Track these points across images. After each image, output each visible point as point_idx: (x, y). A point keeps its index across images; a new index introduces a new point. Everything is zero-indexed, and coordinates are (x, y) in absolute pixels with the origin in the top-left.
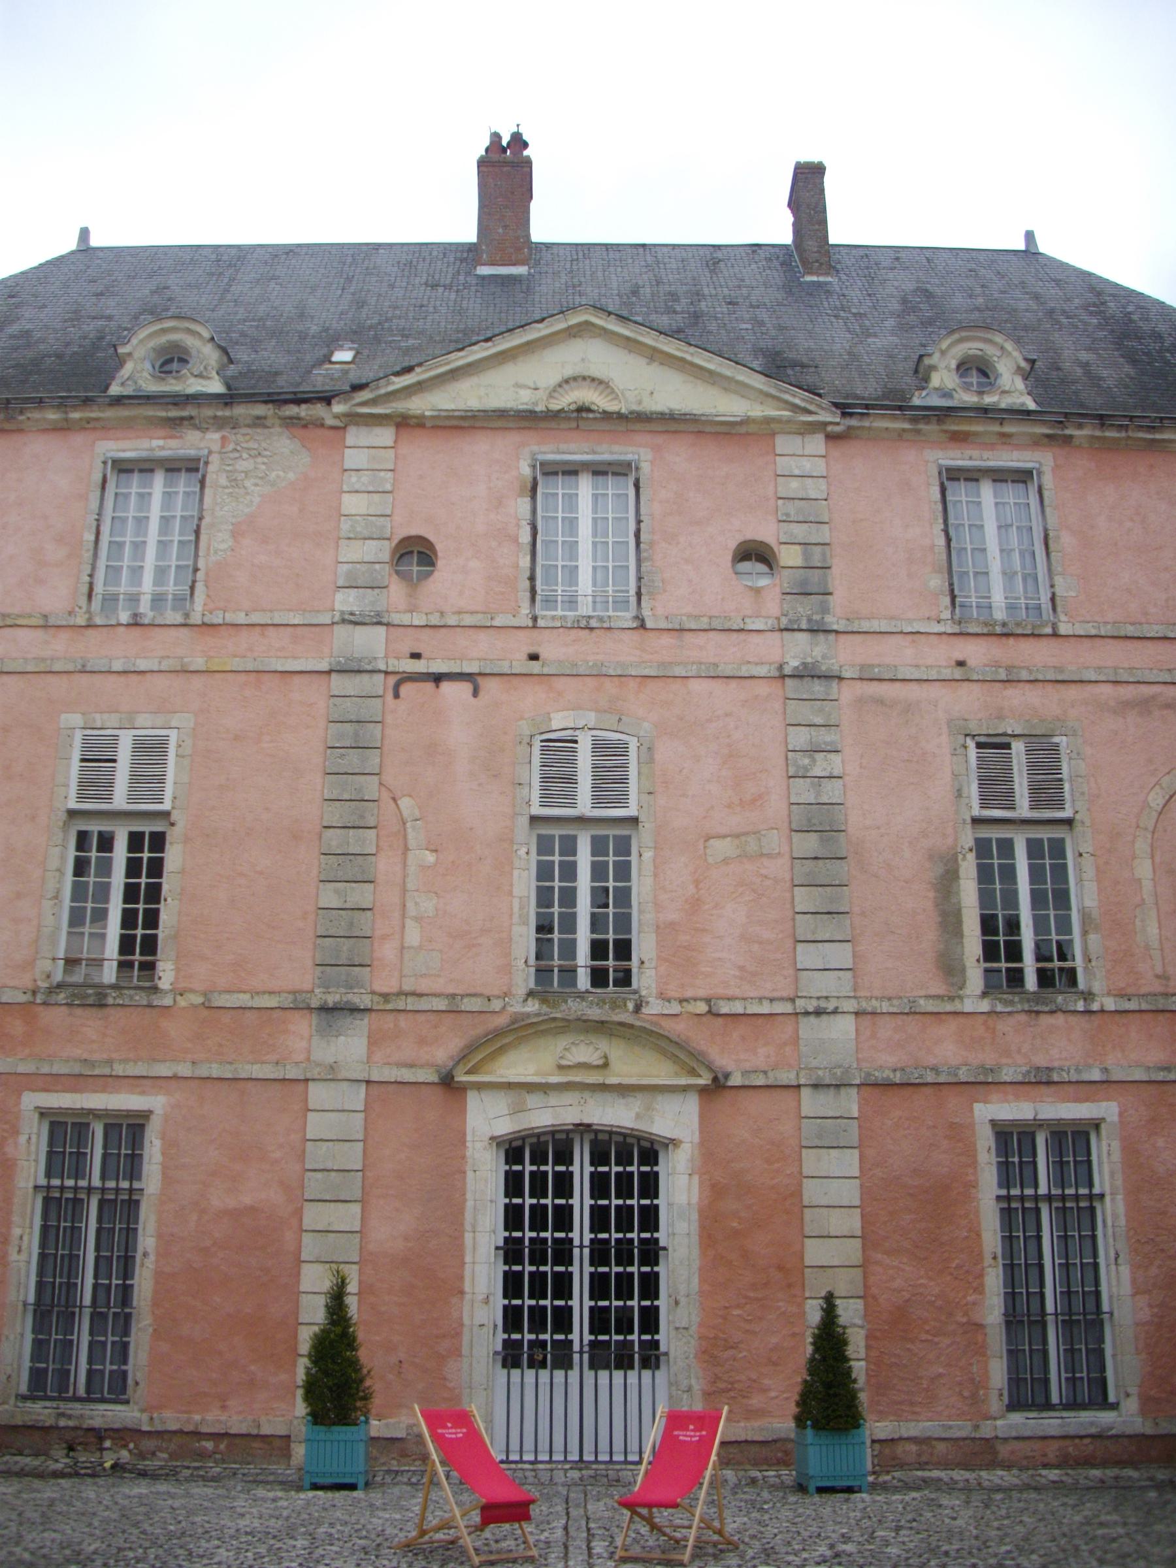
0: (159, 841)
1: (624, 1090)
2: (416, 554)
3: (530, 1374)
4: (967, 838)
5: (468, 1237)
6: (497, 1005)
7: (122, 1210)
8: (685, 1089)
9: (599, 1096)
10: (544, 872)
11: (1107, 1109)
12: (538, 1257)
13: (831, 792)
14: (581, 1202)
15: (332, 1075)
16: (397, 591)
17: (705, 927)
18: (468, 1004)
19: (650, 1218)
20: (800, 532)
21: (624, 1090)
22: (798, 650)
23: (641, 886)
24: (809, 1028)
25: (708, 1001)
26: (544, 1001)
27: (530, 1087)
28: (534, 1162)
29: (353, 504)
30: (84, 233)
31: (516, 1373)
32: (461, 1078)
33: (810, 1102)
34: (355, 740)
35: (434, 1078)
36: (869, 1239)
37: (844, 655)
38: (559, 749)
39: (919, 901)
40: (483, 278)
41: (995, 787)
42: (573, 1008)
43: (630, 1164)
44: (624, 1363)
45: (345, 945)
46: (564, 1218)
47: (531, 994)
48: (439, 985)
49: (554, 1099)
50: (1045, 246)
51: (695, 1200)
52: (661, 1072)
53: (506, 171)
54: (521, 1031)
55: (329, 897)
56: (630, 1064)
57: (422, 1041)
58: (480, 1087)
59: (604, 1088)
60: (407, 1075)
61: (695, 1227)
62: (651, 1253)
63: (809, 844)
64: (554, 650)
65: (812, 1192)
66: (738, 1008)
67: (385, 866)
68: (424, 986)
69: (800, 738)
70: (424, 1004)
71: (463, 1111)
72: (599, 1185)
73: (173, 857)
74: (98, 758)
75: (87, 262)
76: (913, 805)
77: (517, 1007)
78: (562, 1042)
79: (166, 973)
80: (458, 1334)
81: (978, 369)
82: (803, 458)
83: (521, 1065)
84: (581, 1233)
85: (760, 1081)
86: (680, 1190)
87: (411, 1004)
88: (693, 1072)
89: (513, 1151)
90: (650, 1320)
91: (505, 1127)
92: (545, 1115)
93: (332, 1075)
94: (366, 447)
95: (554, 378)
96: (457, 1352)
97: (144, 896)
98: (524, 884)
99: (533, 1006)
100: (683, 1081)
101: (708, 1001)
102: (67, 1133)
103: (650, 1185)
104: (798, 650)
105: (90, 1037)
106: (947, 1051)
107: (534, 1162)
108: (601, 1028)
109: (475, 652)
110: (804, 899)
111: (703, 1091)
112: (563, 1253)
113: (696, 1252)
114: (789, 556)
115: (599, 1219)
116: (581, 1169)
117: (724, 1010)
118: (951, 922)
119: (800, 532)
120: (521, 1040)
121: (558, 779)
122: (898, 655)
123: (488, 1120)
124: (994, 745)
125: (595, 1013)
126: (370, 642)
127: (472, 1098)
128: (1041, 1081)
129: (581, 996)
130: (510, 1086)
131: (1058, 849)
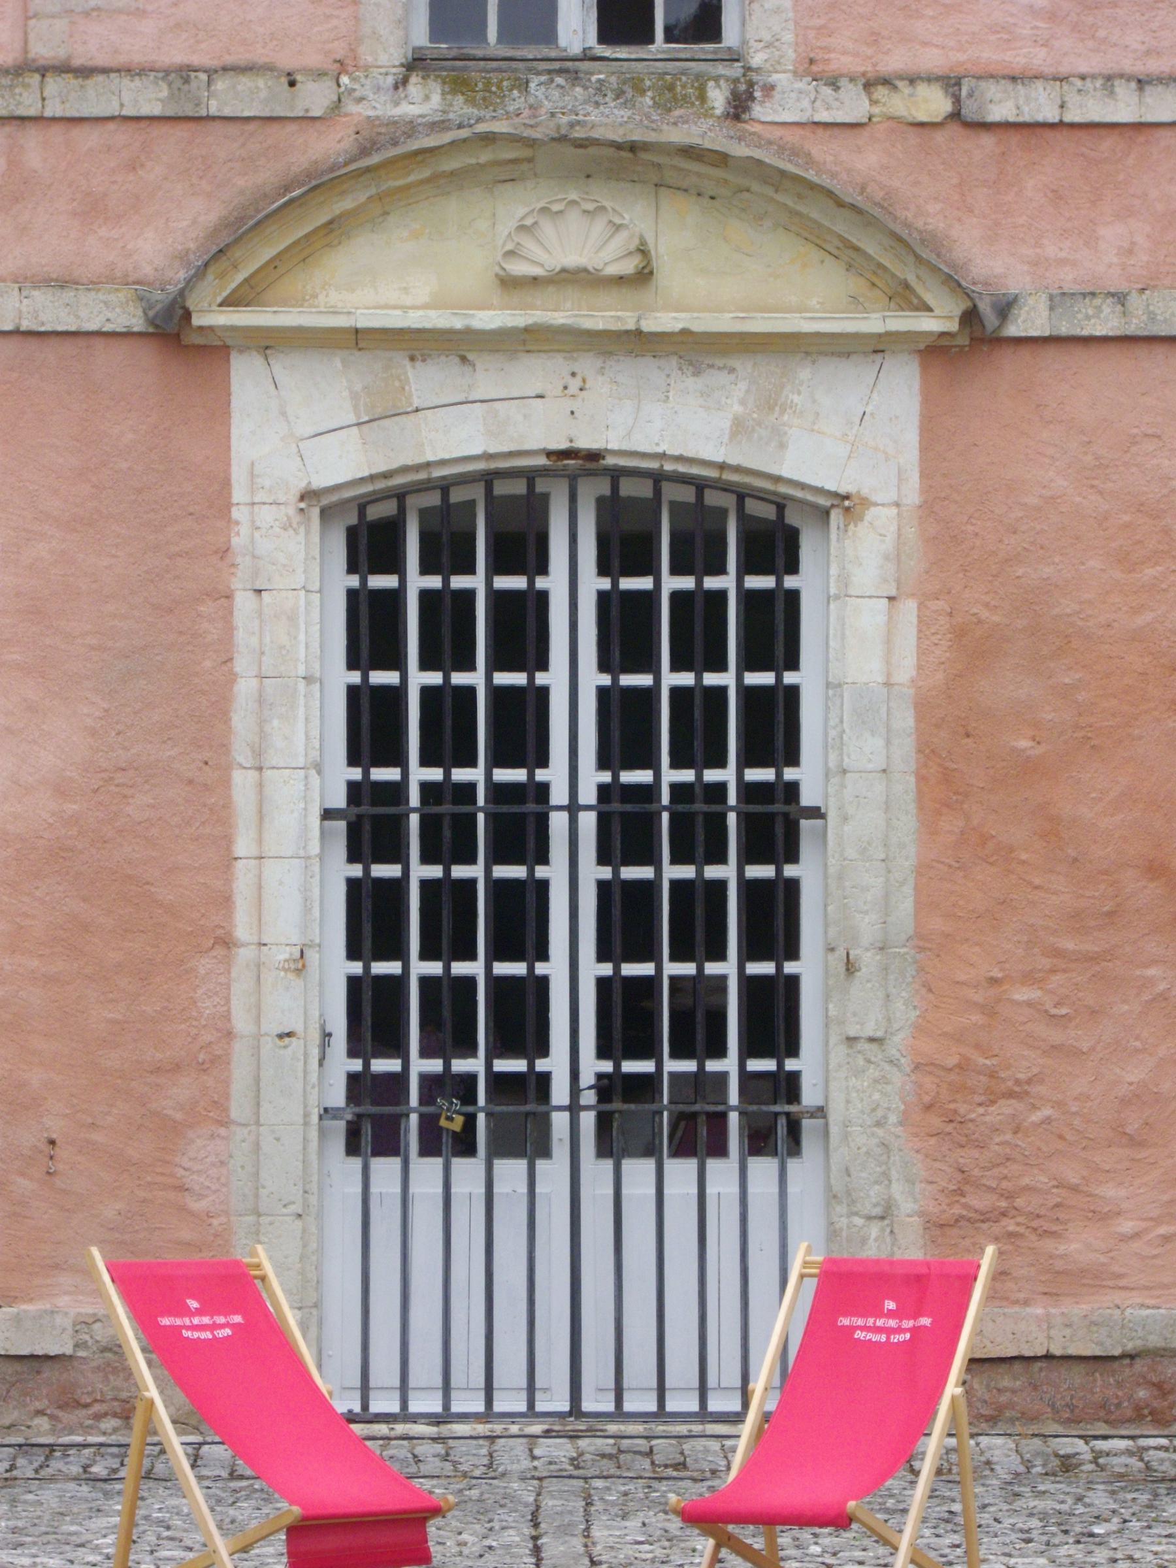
1: (696, 350)
3: (427, 1172)
5: (242, 782)
6: (315, 97)
8: (878, 347)
9: (628, 371)
12: (448, 838)
14: (572, 679)
18: (227, 97)
19: (773, 726)
21: (696, 350)
25: (951, 83)
26: (458, 85)
27: (418, 344)
28: (431, 569)
31: (386, 1169)
32: (211, 316)
35: (133, 319)
42: (546, 104)
43: (714, 571)
44: (698, 1136)
46: (521, 726)
47: (417, 63)
48: (137, 46)
49: (488, 379)
51: (906, 669)
52: (806, 294)
54: (385, 176)
56: (716, 274)
57: (93, 210)
58: (268, 343)
59: (639, 343)
60: (50, 311)
61: (905, 750)
62: (776, 825)
66: (1041, 105)
68: (92, 46)
70: (96, 99)
71: (219, 413)
72: (625, 631)
77: (377, 105)
78: (514, 206)
80: (213, 1062)
83: (390, 277)
84: (572, 770)
85: (1106, 322)
86: (860, 645)
87: (60, 96)
88: (904, 297)
90: (773, 1017)
91: (347, 461)
92: (462, 428)
96: (214, 1112)
99: (424, 101)
100: (873, 324)
101: (951, 83)
103: (774, 631)
111: (934, 352)
112: (521, 827)
113: (907, 823)
115: (625, 728)
116: (572, 585)
117: (1000, 112)
120: (385, 205)
123: (296, 443)
125: (611, 120)
127: (247, 378)
129: (569, 68)
130: (358, 339)
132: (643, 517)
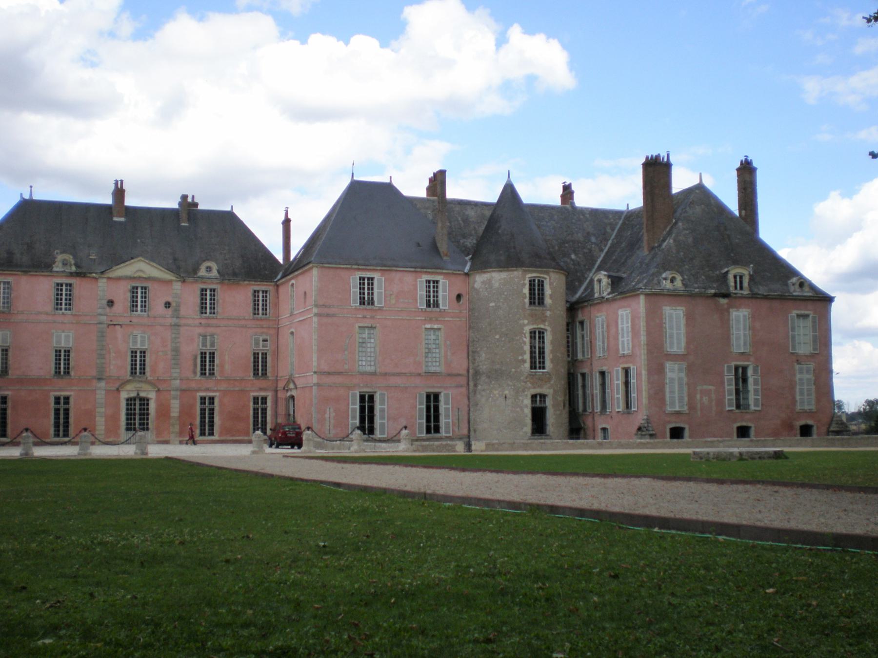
0: (69, 351)
2: (111, 303)
7: (67, 411)
10: (132, 356)
11: (217, 394)
13: (178, 345)
16: (108, 309)
19: (148, 409)
20: (176, 299)
23: (147, 359)
30: (21, 194)
33: (173, 393)
37: (182, 322)
38: (135, 337)
40: (115, 222)
41: (204, 345)
42: (137, 379)
43: (144, 402)
50: (235, 211)
53: (119, 192)
54: (128, 381)
56: (145, 386)
62: (148, 414)
63: (174, 353)
64: (135, 320)
65: (172, 406)
69: (173, 336)
76: (192, 348)
79: (72, 373)
81: (209, 269)
82: (177, 286)
83: (129, 387)
86: (152, 406)
89: (127, 400)
90: (148, 424)
94: (102, 283)
97: (67, 360)
98: (129, 359)
102: (57, 400)
103: (148, 404)
106: (193, 385)
107: (130, 401)
109: (121, 321)
110: (173, 362)
114: (173, 304)
118: (195, 366)
119: (176, 299)
121: (135, 342)
122: (190, 322)
123: (124, 395)
124: (205, 337)
128: (207, 390)
131: (214, 353)
132: (142, 399)
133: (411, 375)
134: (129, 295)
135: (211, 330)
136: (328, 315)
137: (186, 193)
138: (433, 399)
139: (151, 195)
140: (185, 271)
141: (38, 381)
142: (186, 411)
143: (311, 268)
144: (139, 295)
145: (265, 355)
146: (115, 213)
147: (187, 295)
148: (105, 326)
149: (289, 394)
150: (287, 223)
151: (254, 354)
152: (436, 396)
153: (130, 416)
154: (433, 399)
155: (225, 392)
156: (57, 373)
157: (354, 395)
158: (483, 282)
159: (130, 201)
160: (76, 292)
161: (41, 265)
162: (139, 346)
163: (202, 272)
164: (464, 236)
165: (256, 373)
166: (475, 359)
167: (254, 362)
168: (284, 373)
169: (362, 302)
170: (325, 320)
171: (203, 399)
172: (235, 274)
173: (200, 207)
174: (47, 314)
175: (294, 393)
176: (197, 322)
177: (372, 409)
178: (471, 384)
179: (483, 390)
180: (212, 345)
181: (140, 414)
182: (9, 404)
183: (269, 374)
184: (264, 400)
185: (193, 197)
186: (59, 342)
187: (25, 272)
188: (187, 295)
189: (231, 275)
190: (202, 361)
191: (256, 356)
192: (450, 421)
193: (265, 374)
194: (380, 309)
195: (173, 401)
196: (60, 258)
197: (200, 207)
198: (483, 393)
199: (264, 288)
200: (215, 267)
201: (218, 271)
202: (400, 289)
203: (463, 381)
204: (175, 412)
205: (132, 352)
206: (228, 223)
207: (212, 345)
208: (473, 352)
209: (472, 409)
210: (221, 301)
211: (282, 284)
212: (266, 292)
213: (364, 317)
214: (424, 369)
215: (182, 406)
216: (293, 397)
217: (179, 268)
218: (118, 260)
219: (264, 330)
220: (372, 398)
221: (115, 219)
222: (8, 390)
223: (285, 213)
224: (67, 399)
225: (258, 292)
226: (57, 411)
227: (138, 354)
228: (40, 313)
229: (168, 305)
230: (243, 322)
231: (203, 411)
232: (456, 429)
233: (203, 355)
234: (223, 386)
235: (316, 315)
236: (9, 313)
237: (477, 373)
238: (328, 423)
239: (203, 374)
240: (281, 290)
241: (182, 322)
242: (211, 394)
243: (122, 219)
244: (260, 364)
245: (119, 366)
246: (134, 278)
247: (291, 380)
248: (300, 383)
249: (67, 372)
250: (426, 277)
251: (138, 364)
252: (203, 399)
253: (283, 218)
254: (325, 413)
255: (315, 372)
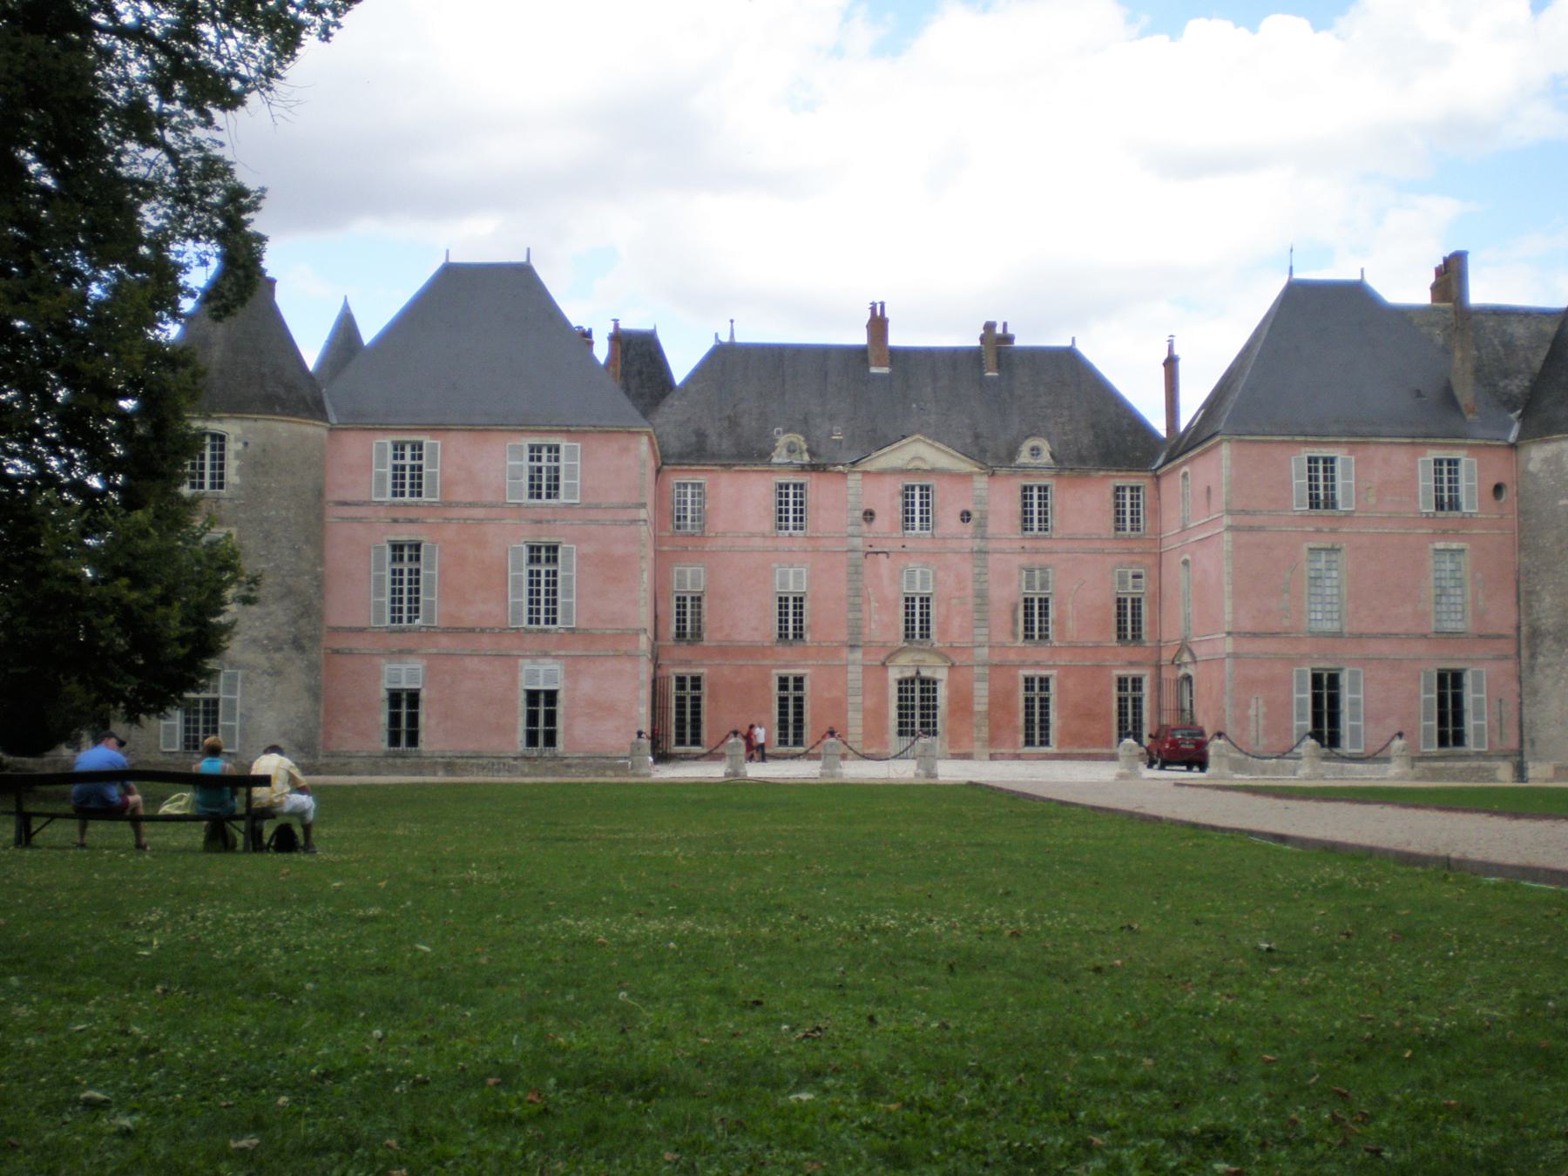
0: (801, 599)
2: (869, 515)
4: (1021, 599)
7: (799, 701)
11: (1053, 672)
15: (854, 663)
16: (865, 526)
17: (949, 622)
19: (935, 699)
22: (977, 544)
23: (932, 611)
24: (978, 651)
29: (851, 499)
33: (977, 670)
34: (856, 570)
36: (990, 704)
37: (992, 545)
38: (911, 574)
39: (1007, 617)
40: (875, 375)
41: (1030, 585)
43: (928, 685)
45: (856, 628)
53: (878, 325)
54: (901, 650)
55: (850, 616)
56: (930, 659)
62: (935, 707)
63: (979, 601)
64: (909, 544)
65: (976, 693)
67: (865, 607)
69: (977, 570)
73: (806, 604)
74: (784, 575)
75: (727, 361)
76: (1007, 592)
79: (807, 637)
81: (1035, 451)
82: (981, 483)
83: (903, 660)
86: (942, 693)
89: (900, 682)
90: (935, 724)
91: (899, 676)
93: (854, 663)
94: (854, 480)
95: (908, 457)
97: (799, 616)
98: (902, 611)
103: (935, 690)
104: (977, 544)
105: (788, 653)
106: (1012, 657)
108: (923, 650)
109: (888, 546)
110: (976, 616)
114: (975, 515)
118: (1015, 622)
121: (911, 582)
123: (894, 674)
124: (1030, 571)
126: (858, 542)
128: (1037, 665)
131: (1047, 600)
133: (1408, 636)
134: (899, 500)
135: (1040, 559)
136: (1251, 529)
137: (991, 319)
138: (1450, 684)
139: (934, 322)
140: (993, 455)
141: (752, 651)
142: (999, 702)
143: (1219, 444)
144: (916, 502)
145: (1136, 602)
146: (872, 359)
147: (999, 498)
148: (861, 555)
149: (1182, 672)
150: (1171, 364)
151: (1119, 600)
152: (1457, 677)
153: (904, 709)
154: (1450, 684)
155: (1067, 670)
156: (783, 636)
157: (1301, 675)
158: (1545, 461)
159: (897, 338)
160: (811, 497)
161: (752, 454)
162: (918, 589)
163: (1024, 457)
164: (1506, 375)
165: (1121, 636)
166: (1531, 607)
167: (1119, 615)
168: (1171, 633)
169: (1314, 503)
170: (1246, 538)
171: (1029, 682)
172: (1082, 460)
173: (1017, 343)
174: (764, 536)
175: (1190, 670)
176: (1017, 545)
177: (1334, 701)
178: (1525, 653)
179: (1549, 665)
180: (1044, 585)
181: (922, 708)
182: (705, 689)
183: (1144, 637)
184: (1137, 683)
185: (1005, 325)
186: (784, 584)
187: (727, 467)
188: (999, 498)
189: (1072, 463)
190: (1026, 615)
191: (1121, 602)
192: (1485, 723)
193: (1137, 637)
194: (1348, 515)
195: (977, 685)
196: (783, 440)
197: (1017, 343)
198: (1549, 671)
199: (1134, 482)
200: (1045, 447)
201: (1052, 455)
202: (1384, 478)
203: (1508, 647)
204: (981, 704)
205: (907, 600)
206: (1066, 371)
207: (1044, 585)
208: (1529, 593)
209: (1526, 702)
210: (1057, 508)
211: (1167, 473)
212: (1138, 489)
213: (1319, 531)
214: (1433, 626)
215: (993, 694)
216: (1188, 678)
217: (983, 451)
218: (880, 442)
219: (1137, 558)
220: (1334, 680)
221: (873, 370)
222: (702, 666)
223: (1166, 344)
224: (799, 681)
225: (1124, 488)
226: (783, 701)
227: (917, 604)
228: (753, 535)
229: (966, 516)
230: (1098, 545)
231: (1029, 702)
232: (1496, 739)
233: (1028, 602)
234: (1064, 659)
235: (1229, 528)
236: (703, 536)
237: (1535, 634)
238: (1252, 725)
239: (1028, 637)
240: (1164, 483)
241: (992, 545)
242: (1044, 673)
243: (885, 370)
244: (1128, 620)
245: (885, 624)
246: (908, 471)
247: (1184, 646)
248: (1201, 652)
249: (799, 636)
250: (1433, 454)
251: (917, 620)
252: (1029, 682)
253: (1165, 356)
254: (1248, 706)
255: (1229, 633)
